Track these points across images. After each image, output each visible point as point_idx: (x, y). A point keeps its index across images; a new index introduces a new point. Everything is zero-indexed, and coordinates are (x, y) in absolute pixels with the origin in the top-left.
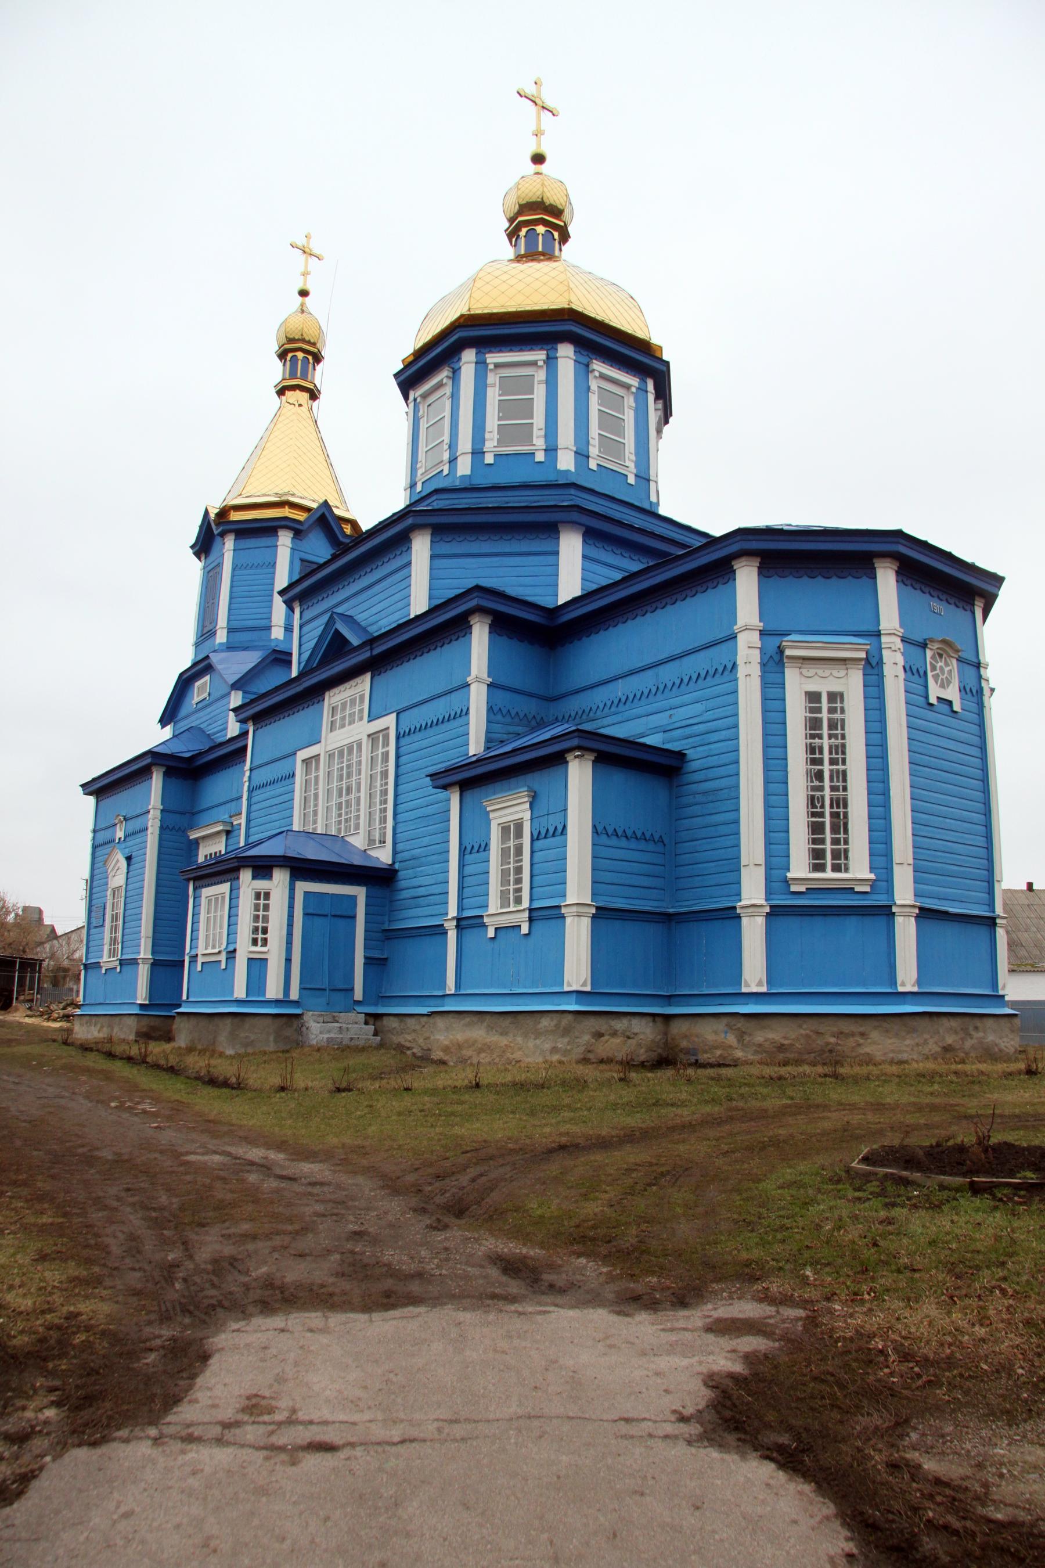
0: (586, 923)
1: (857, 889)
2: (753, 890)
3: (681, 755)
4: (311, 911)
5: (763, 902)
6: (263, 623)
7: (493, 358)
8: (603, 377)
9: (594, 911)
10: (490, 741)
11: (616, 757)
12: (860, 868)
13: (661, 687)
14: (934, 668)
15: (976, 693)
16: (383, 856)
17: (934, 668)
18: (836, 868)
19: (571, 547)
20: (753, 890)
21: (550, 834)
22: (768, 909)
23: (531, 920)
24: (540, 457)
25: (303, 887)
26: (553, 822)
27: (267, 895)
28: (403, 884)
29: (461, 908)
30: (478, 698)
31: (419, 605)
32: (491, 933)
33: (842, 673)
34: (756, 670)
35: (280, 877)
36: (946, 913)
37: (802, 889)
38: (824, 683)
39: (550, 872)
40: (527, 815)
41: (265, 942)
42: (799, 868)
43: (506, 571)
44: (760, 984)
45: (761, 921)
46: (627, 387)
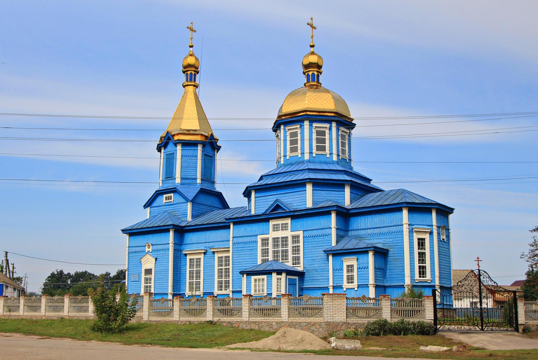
3: (388, 250)
6: (194, 177)
7: (315, 125)
8: (343, 131)
15: (448, 236)
16: (300, 268)
21: (363, 268)
24: (328, 156)
25: (288, 277)
27: (280, 279)
28: (306, 276)
29: (333, 283)
32: (345, 289)
35: (284, 275)
46: (347, 133)
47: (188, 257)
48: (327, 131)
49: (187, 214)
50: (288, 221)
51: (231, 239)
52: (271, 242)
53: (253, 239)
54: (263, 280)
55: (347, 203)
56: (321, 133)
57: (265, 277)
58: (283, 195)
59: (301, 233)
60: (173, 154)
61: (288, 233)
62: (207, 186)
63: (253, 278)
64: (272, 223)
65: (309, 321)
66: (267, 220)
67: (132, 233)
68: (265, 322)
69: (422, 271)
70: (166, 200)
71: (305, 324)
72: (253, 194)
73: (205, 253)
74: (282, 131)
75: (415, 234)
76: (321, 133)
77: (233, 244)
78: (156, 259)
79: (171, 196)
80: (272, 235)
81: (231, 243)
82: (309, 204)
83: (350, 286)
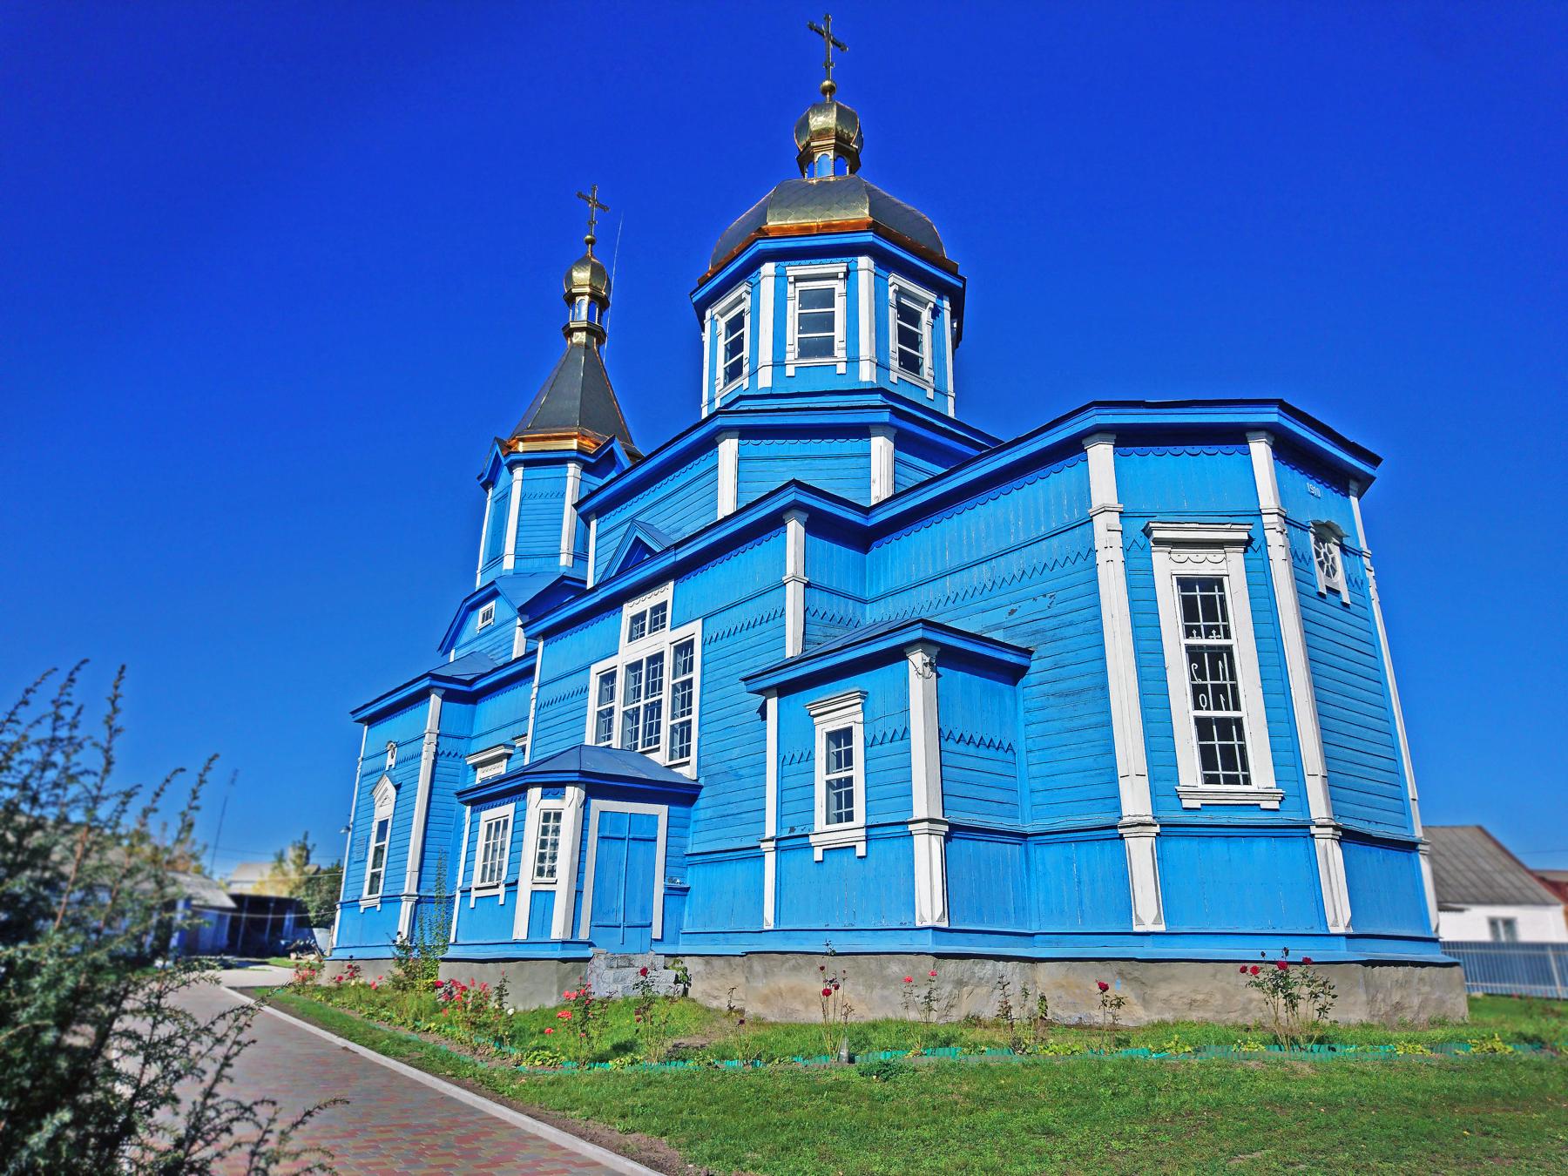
0: (937, 843)
1: (1264, 805)
4: (607, 834)
5: (1149, 819)
7: (794, 270)
9: (946, 828)
11: (958, 656)
13: (999, 582)
14: (1318, 555)
16: (688, 773)
17: (1318, 555)
19: (881, 448)
22: (1157, 829)
23: (867, 840)
24: (841, 368)
25: (597, 805)
27: (558, 816)
30: (793, 596)
31: (726, 505)
32: (818, 854)
33: (1220, 557)
34: (1118, 556)
35: (573, 794)
36: (1369, 836)
37: (1197, 804)
39: (892, 780)
41: (552, 872)
43: (818, 464)
44: (1155, 923)
45: (1148, 842)
48: (839, 287)
58: (662, 506)
69: (1222, 751)
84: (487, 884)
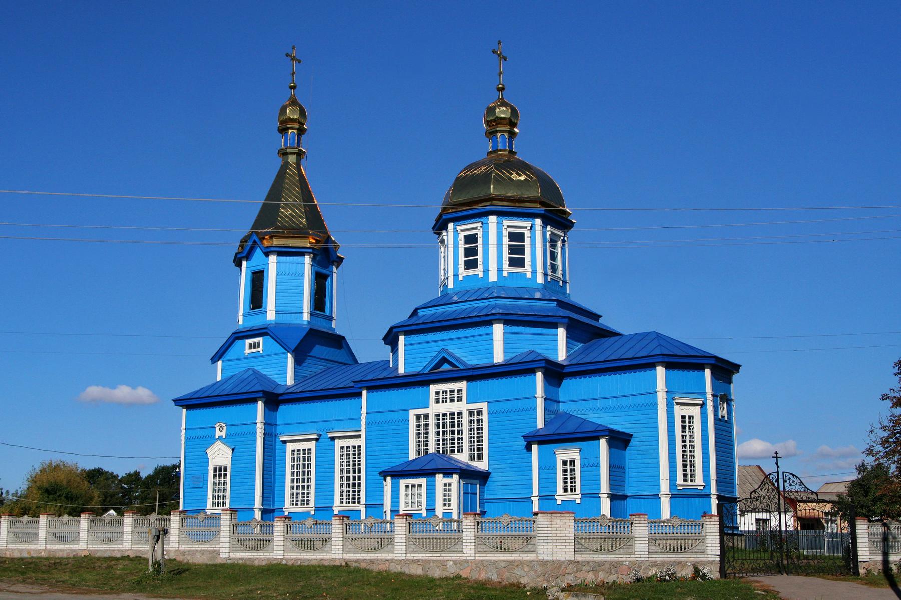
2: (665, 488)
10: (546, 423)
12: (699, 480)
16: (482, 466)
18: (691, 481)
20: (665, 488)
21: (591, 466)
26: (592, 461)
27: (450, 485)
32: (559, 502)
35: (455, 477)
38: (687, 411)
40: (578, 458)
41: (450, 505)
42: (680, 480)
45: (668, 500)
47: (290, 447)
49: (286, 373)
50: (463, 385)
51: (364, 416)
52: (432, 421)
53: (400, 415)
54: (420, 486)
55: (561, 356)
56: (516, 237)
57: (423, 481)
59: (484, 406)
60: (263, 271)
61: (462, 407)
62: (321, 325)
63: (403, 482)
64: (434, 388)
65: (512, 559)
66: (427, 383)
67: (190, 403)
68: (434, 561)
70: (250, 348)
71: (503, 564)
72: (402, 338)
73: (317, 440)
74: (451, 233)
75: (676, 408)
76: (516, 237)
77: (367, 424)
78: (233, 450)
79: (259, 343)
80: (434, 409)
81: (363, 422)
82: (498, 357)
83: (569, 497)
84: (410, 508)
